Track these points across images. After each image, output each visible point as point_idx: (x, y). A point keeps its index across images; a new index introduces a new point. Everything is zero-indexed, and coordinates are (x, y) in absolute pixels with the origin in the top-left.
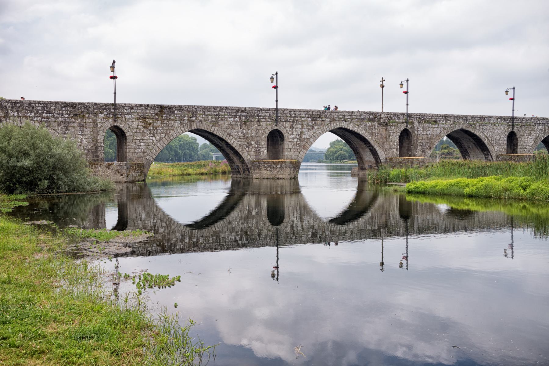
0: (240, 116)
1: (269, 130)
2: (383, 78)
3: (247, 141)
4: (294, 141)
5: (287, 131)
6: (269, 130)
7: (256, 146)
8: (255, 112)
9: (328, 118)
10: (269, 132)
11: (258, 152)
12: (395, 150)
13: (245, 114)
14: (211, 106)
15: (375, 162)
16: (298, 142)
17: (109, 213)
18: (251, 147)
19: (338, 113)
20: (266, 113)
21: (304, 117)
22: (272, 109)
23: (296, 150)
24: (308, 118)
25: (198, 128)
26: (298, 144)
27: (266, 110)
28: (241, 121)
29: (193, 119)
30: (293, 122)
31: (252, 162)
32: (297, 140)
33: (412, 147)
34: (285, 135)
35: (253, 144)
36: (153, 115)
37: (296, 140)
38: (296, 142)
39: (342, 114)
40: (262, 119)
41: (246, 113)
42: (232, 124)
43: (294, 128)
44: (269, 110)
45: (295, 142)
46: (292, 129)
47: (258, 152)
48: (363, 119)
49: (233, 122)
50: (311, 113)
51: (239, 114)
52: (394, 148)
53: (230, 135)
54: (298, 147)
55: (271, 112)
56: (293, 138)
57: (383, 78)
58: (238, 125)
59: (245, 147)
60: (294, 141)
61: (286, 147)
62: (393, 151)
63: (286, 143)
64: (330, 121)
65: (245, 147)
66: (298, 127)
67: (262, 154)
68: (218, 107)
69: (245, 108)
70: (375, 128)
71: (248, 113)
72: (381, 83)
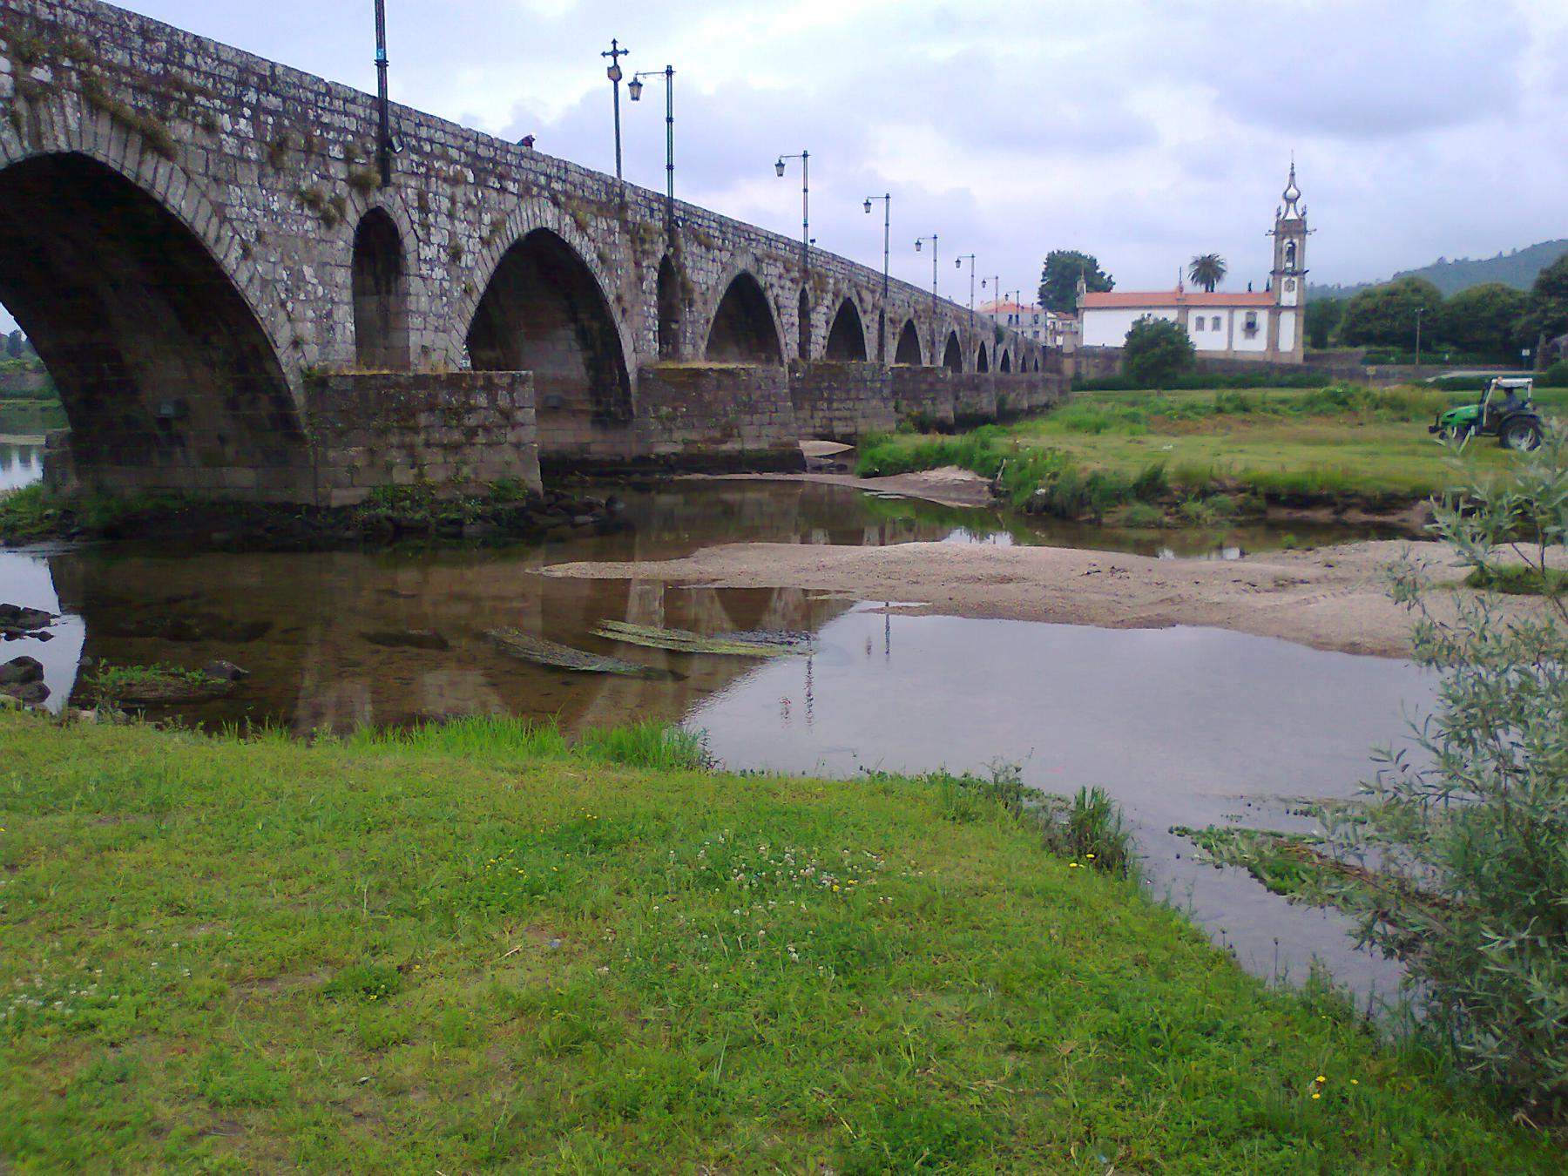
0: (257, 109)
3: (289, 263)
5: (412, 222)
7: (320, 289)
8: (308, 102)
9: (515, 181)
11: (326, 322)
13: (273, 102)
14: (131, 16)
15: (587, 382)
18: (302, 297)
19: (537, 162)
20: (346, 114)
21: (457, 162)
22: (363, 94)
24: (465, 170)
25: (76, 147)
27: (345, 100)
28: (259, 139)
29: (42, 74)
30: (427, 176)
31: (317, 382)
33: (674, 326)
34: (409, 242)
39: (542, 166)
40: (335, 142)
41: (275, 94)
42: (227, 150)
44: (353, 101)
47: (326, 322)
48: (590, 202)
49: (231, 140)
50: (471, 145)
51: (251, 96)
53: (219, 210)
55: (360, 112)
58: (248, 161)
59: (283, 296)
61: (412, 304)
63: (415, 285)
64: (519, 196)
65: (283, 296)
67: (339, 337)
68: (161, 27)
69: (273, 66)
71: (284, 100)
72: (610, 61)
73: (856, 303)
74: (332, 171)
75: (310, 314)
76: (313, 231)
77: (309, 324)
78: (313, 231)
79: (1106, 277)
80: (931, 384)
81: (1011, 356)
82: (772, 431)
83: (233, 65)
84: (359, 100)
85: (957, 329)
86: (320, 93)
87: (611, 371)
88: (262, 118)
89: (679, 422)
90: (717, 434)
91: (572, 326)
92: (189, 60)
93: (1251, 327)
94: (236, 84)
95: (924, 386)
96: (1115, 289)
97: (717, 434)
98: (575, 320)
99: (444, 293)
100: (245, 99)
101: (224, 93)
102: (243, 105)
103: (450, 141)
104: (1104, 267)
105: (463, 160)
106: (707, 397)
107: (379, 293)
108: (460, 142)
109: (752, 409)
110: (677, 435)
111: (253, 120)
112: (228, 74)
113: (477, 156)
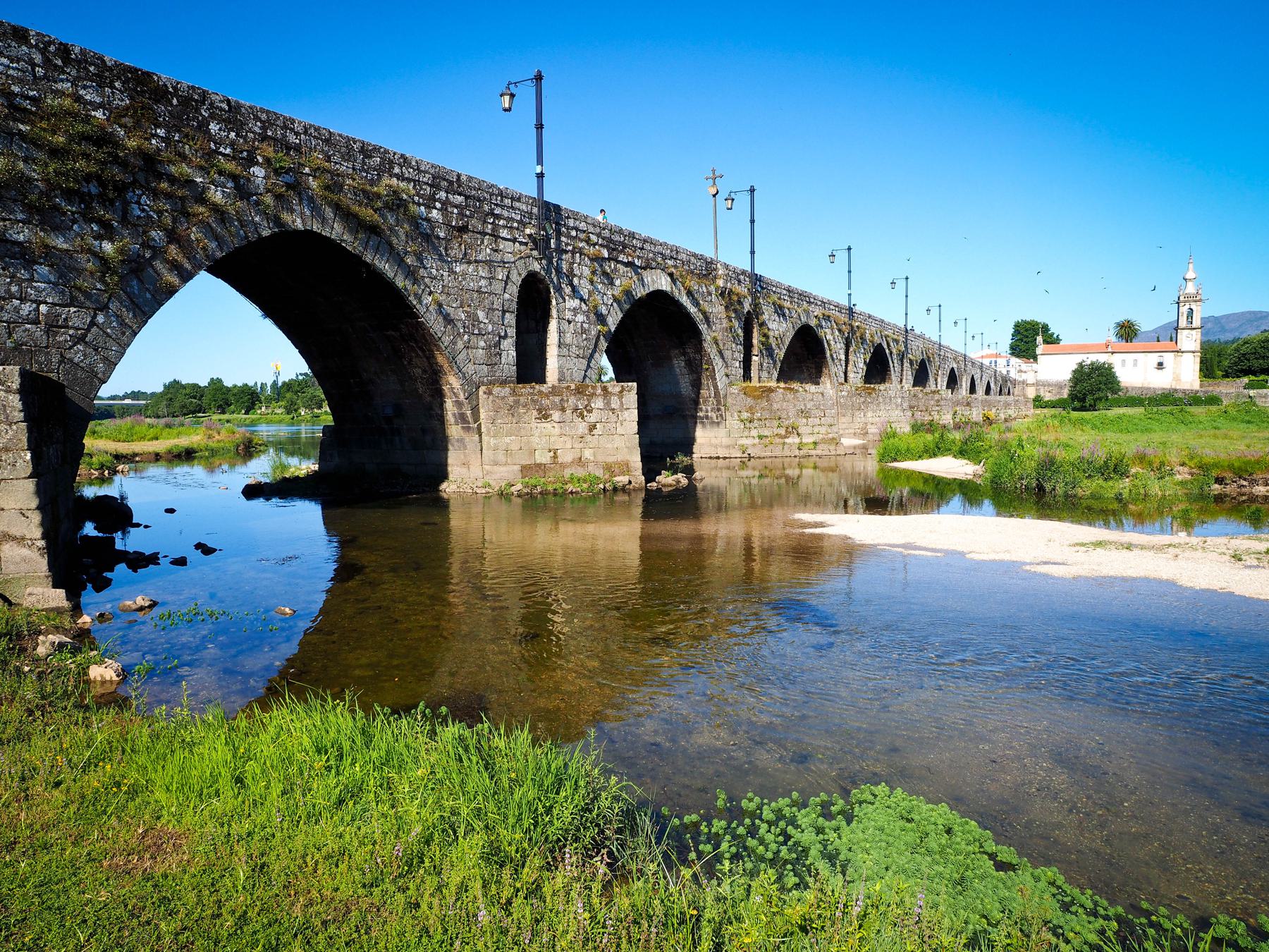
0: (445, 203)
1: (520, 275)
2: (714, 171)
27: (512, 199)
35: (481, 319)
36: (99, 114)
37: (580, 318)
39: (659, 249)
41: (460, 194)
44: (519, 200)
50: (606, 233)
55: (524, 207)
57: (714, 171)
68: (376, 149)
71: (467, 197)
73: (885, 347)
74: (501, 247)
75: (482, 344)
76: (486, 287)
77: (481, 351)
78: (486, 287)
79: (1055, 336)
80: (938, 401)
81: (992, 385)
82: (823, 430)
83: (429, 173)
84: (523, 200)
85: (955, 366)
86: (494, 194)
87: (709, 389)
88: (449, 210)
89: (756, 423)
90: (783, 431)
91: (683, 358)
92: (397, 170)
93: (1160, 366)
94: (431, 186)
95: (932, 402)
96: (1062, 343)
97: (783, 431)
98: (684, 354)
99: (584, 331)
100: (437, 197)
101: (422, 192)
102: (436, 200)
103: (591, 229)
104: (1054, 329)
105: (600, 242)
106: (775, 406)
107: (538, 331)
108: (598, 230)
109: (805, 413)
110: (754, 433)
111: (443, 210)
112: (425, 180)
113: (610, 240)
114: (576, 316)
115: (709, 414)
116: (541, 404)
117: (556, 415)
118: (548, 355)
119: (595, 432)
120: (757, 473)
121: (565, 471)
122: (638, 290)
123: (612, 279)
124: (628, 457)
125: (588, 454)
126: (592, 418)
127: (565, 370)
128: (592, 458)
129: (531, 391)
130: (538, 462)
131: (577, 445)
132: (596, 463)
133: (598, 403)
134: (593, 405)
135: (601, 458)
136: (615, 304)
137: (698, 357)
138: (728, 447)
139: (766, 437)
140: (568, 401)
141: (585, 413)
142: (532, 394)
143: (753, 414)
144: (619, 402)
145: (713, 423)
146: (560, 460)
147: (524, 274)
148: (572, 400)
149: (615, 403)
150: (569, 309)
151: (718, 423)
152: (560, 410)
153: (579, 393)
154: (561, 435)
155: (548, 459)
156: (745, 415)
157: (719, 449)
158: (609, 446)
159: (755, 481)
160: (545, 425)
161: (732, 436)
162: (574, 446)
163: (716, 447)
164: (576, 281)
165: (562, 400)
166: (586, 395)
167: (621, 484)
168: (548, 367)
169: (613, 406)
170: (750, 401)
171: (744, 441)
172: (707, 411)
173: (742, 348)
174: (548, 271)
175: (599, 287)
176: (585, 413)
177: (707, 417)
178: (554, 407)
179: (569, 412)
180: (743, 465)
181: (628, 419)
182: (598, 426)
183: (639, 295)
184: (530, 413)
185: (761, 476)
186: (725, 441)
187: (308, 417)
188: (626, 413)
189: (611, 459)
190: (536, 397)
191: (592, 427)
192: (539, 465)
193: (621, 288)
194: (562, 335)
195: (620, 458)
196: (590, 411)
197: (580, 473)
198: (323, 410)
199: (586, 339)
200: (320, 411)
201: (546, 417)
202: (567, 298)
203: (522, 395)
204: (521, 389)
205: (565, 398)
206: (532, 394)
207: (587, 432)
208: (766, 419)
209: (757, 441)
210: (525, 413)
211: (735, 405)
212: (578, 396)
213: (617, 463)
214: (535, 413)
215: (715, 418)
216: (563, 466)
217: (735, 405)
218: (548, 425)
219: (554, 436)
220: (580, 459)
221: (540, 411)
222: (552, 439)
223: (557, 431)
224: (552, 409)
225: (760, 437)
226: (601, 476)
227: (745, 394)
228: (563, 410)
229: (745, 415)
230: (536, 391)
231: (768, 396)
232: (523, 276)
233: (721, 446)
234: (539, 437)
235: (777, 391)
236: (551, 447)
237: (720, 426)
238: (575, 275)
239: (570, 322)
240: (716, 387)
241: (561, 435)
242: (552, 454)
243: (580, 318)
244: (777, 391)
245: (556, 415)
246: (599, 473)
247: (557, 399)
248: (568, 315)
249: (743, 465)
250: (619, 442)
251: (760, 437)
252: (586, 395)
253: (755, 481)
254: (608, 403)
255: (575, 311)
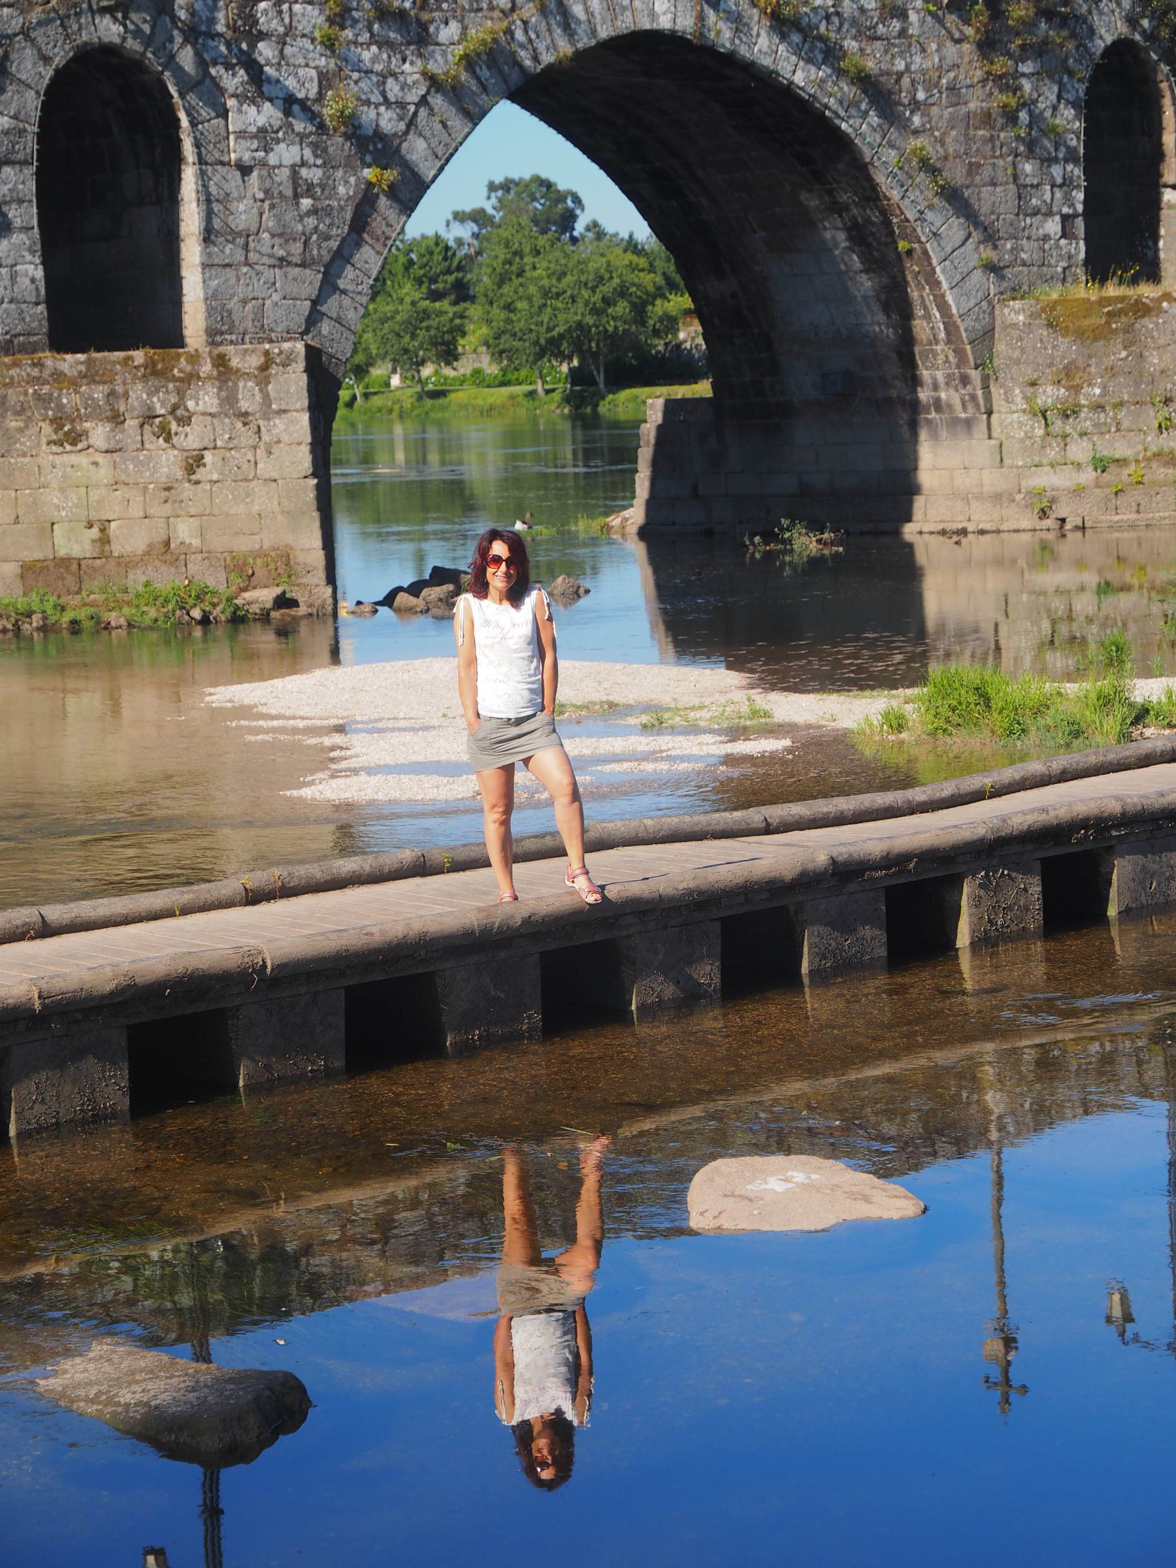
1: (46, 60)
4: (272, 159)
6: (46, 60)
10: (48, 73)
12: (1053, 226)
16: (304, 172)
17: (24, 988)
23: (297, 248)
26: (309, 191)
32: (295, 149)
38: (294, 170)
43: (262, 36)
45: (284, 175)
46: (253, 46)
52: (1050, 214)
54: (311, 222)
56: (262, 130)
60: (272, 159)
62: (1046, 238)
66: (302, 26)
70: (903, 33)
87: (928, 316)
89: (1086, 419)
99: (300, 188)
106: (1154, 360)
110: (1080, 450)
114: (268, 150)
115: (943, 395)
116: (60, 407)
117: (99, 433)
118: (185, 272)
119: (201, 474)
120: (1091, 579)
121: (131, 576)
122: (541, 47)
123: (424, 26)
124: (289, 539)
125: (185, 532)
126: (191, 438)
127: (233, 304)
128: (196, 542)
129: (35, 372)
130: (62, 553)
131: (157, 510)
132: (207, 555)
133: (205, 399)
134: (191, 404)
135: (218, 543)
136: (437, 101)
137: (875, 217)
138: (997, 498)
139: (1121, 462)
140: (126, 395)
141: (174, 426)
142: (32, 381)
143: (1077, 389)
144: (258, 397)
145: (954, 422)
146: (116, 548)
147: (61, 55)
148: (138, 393)
149: (248, 397)
150: (242, 134)
151: (968, 424)
152: (108, 419)
153: (155, 373)
154: (116, 484)
155: (87, 545)
156: (1049, 394)
157: (975, 505)
158: (240, 509)
159: (1084, 604)
160: (75, 459)
161: (1007, 462)
162: (151, 511)
163: (965, 498)
164: (265, 51)
165: (112, 394)
166: (174, 379)
167: (255, 609)
168: (185, 299)
169: (244, 405)
170: (1066, 348)
171: (1046, 479)
172: (936, 387)
173: (1077, 172)
174: (157, 41)
175: (366, 55)
176: (174, 426)
177: (938, 405)
178: (94, 413)
179: (131, 423)
180: (1045, 554)
181: (285, 438)
182: (208, 457)
183: (547, 58)
184: (33, 430)
185: (1106, 588)
186: (992, 480)
187: (408, 396)
188: (279, 424)
189: (244, 545)
190: (46, 389)
191: (194, 463)
192: (65, 562)
193: (460, 50)
194: (216, 207)
195: (267, 540)
196: (185, 421)
197: (167, 580)
198: (465, 367)
199: (314, 211)
200: (448, 372)
201: (74, 438)
202: (231, 103)
203: (11, 384)
204: (9, 367)
205: (120, 389)
206: (32, 381)
207: (180, 474)
208: (1121, 404)
209: (1088, 476)
210: (21, 430)
211: (1018, 362)
212: (153, 382)
213: (260, 554)
214: (47, 429)
215: (958, 406)
216: (126, 564)
217: (1018, 362)
218: (82, 460)
219: (98, 486)
220: (167, 543)
221: (58, 423)
222: (94, 495)
223: (104, 474)
224: (88, 418)
225: (1102, 465)
226: (222, 588)
227: (1050, 325)
228: (117, 419)
229: (1049, 394)
230: (46, 374)
231: (1130, 328)
232: (59, 60)
233: (980, 497)
234: (62, 490)
235: (1161, 311)
236: (94, 516)
237: (975, 430)
238: (262, 36)
239: (245, 170)
240: (943, 307)
241: (116, 484)
242: (95, 532)
243: (286, 154)
244: (1161, 311)
245: (99, 433)
246: (216, 580)
247: (99, 393)
248: (239, 151)
249: (1045, 554)
250: (263, 500)
251: (1102, 465)
252: (174, 379)
253: (1084, 604)
254: (229, 400)
255: (265, 137)
